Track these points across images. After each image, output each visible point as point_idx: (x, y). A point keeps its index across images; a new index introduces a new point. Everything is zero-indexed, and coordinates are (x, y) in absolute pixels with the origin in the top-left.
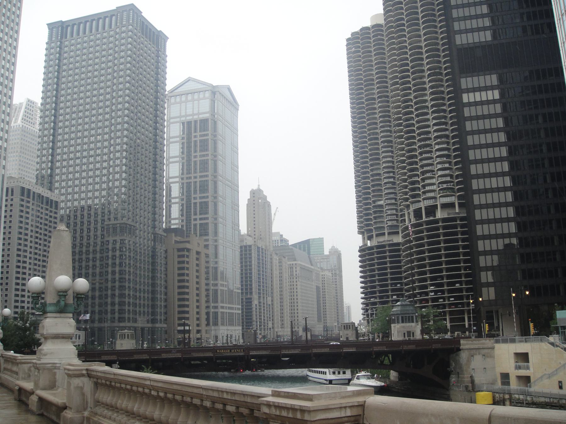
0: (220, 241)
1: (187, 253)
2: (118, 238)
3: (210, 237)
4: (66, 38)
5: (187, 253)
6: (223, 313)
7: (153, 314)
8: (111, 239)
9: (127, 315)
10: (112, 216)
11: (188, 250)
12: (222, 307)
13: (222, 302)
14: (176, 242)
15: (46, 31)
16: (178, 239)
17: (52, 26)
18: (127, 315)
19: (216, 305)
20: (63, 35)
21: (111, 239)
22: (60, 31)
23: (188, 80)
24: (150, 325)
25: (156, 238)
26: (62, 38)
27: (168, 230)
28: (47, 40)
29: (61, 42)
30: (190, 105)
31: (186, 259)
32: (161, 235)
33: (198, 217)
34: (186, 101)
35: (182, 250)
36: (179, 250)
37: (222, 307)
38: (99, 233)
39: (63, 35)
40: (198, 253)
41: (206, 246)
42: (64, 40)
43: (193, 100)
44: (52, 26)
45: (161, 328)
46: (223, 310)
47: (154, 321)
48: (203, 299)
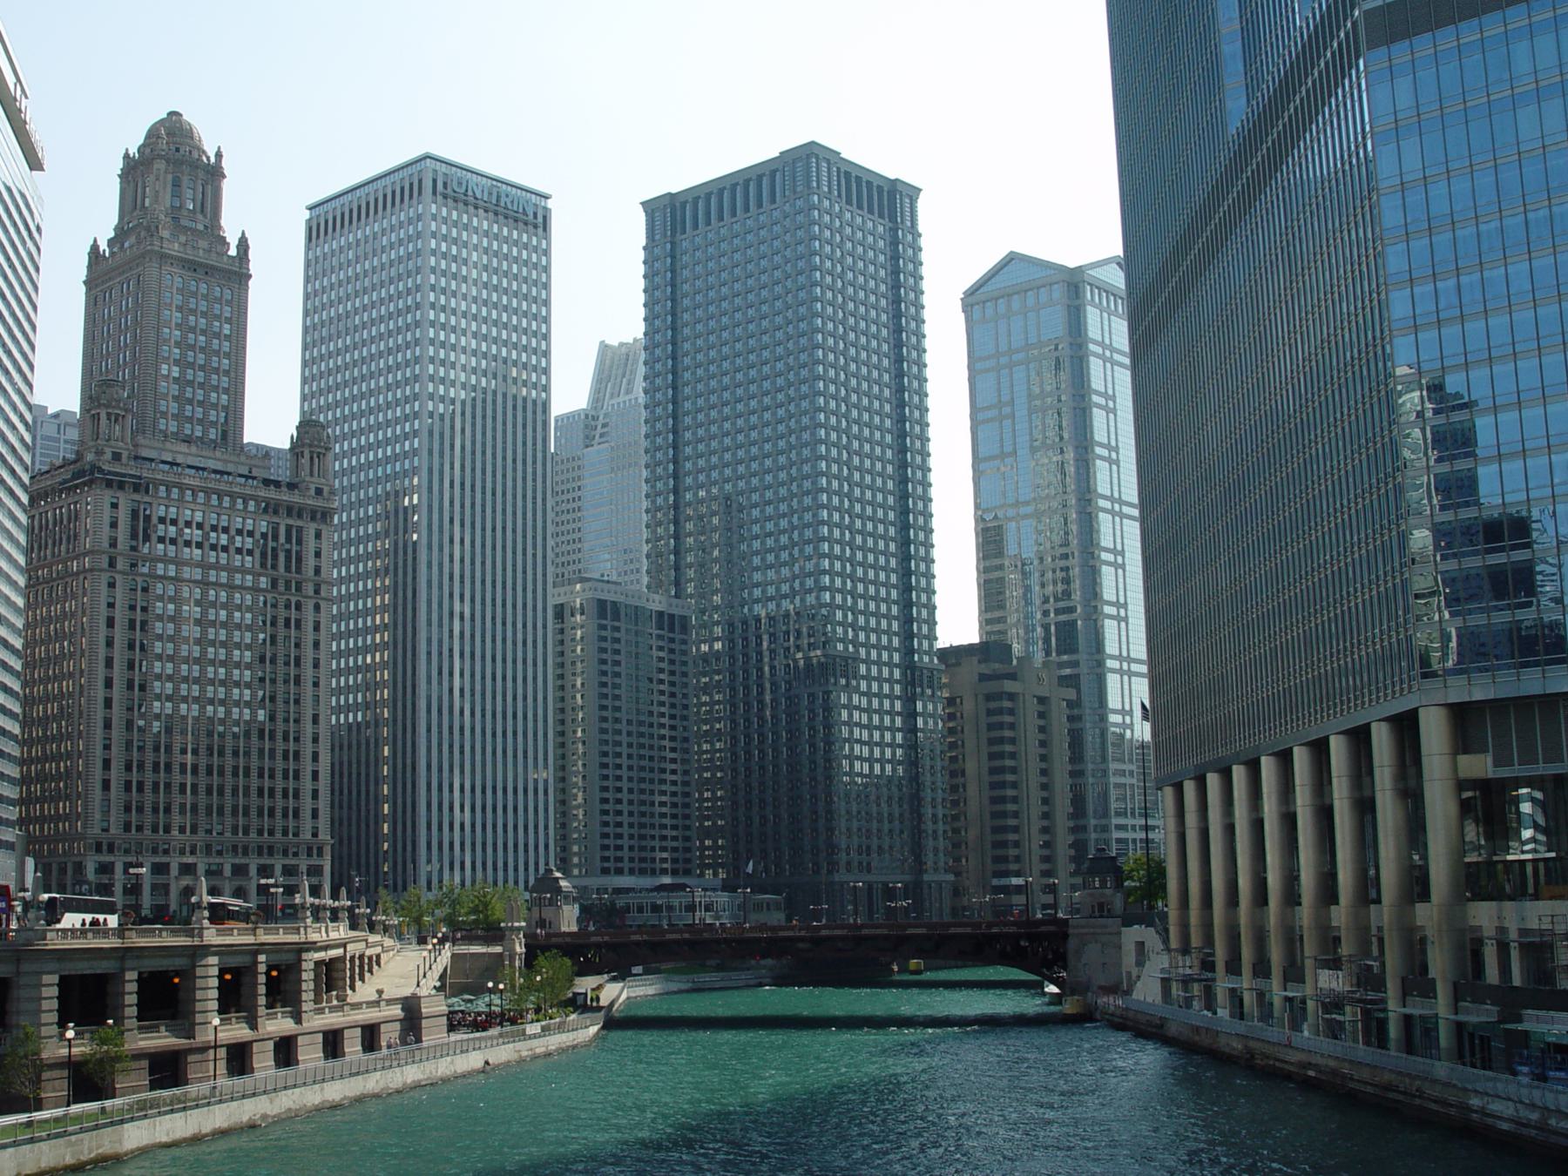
0: (1110, 663)
1: (1007, 704)
3: (1082, 657)
4: (684, 232)
5: (1007, 704)
6: (1119, 841)
11: (1012, 697)
12: (1120, 827)
15: (640, 220)
17: (650, 207)
19: (1103, 822)
22: (672, 220)
25: (914, 678)
26: (673, 234)
27: (954, 656)
28: (643, 242)
29: (673, 244)
31: (1008, 719)
32: (931, 671)
35: (999, 696)
36: (989, 697)
37: (1120, 827)
40: (1042, 700)
41: (1072, 681)
42: (679, 237)
44: (650, 207)
45: (939, 884)
46: (1122, 835)
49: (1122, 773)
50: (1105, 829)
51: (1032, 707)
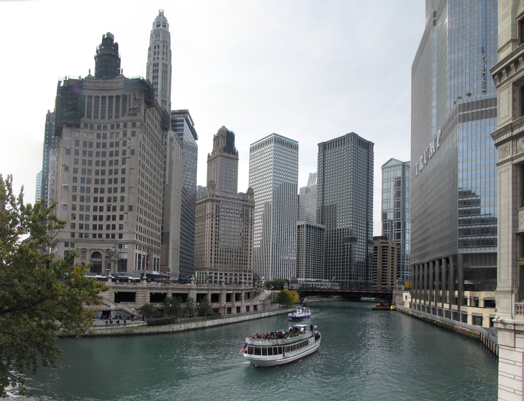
2: (349, 244)
7: (367, 276)
8: (346, 244)
9: (352, 277)
10: (347, 234)
11: (387, 247)
13: (407, 270)
14: (382, 243)
15: (317, 147)
16: (382, 241)
17: (319, 145)
18: (352, 277)
20: (325, 149)
21: (346, 244)
22: (324, 147)
23: (391, 160)
24: (365, 281)
25: (368, 242)
27: (376, 238)
30: (392, 173)
33: (396, 230)
34: (391, 170)
36: (383, 247)
38: (342, 241)
39: (325, 149)
40: (393, 248)
43: (394, 170)
44: (319, 145)
47: (367, 279)
48: (395, 269)
49: (407, 263)
50: (404, 273)
51: (391, 249)
